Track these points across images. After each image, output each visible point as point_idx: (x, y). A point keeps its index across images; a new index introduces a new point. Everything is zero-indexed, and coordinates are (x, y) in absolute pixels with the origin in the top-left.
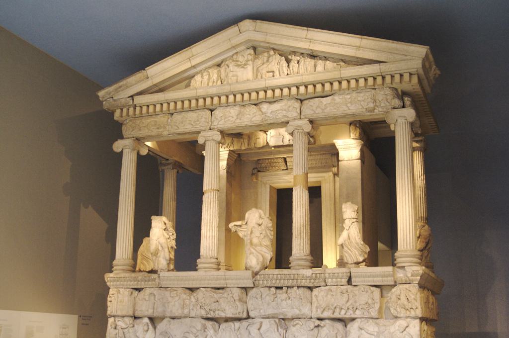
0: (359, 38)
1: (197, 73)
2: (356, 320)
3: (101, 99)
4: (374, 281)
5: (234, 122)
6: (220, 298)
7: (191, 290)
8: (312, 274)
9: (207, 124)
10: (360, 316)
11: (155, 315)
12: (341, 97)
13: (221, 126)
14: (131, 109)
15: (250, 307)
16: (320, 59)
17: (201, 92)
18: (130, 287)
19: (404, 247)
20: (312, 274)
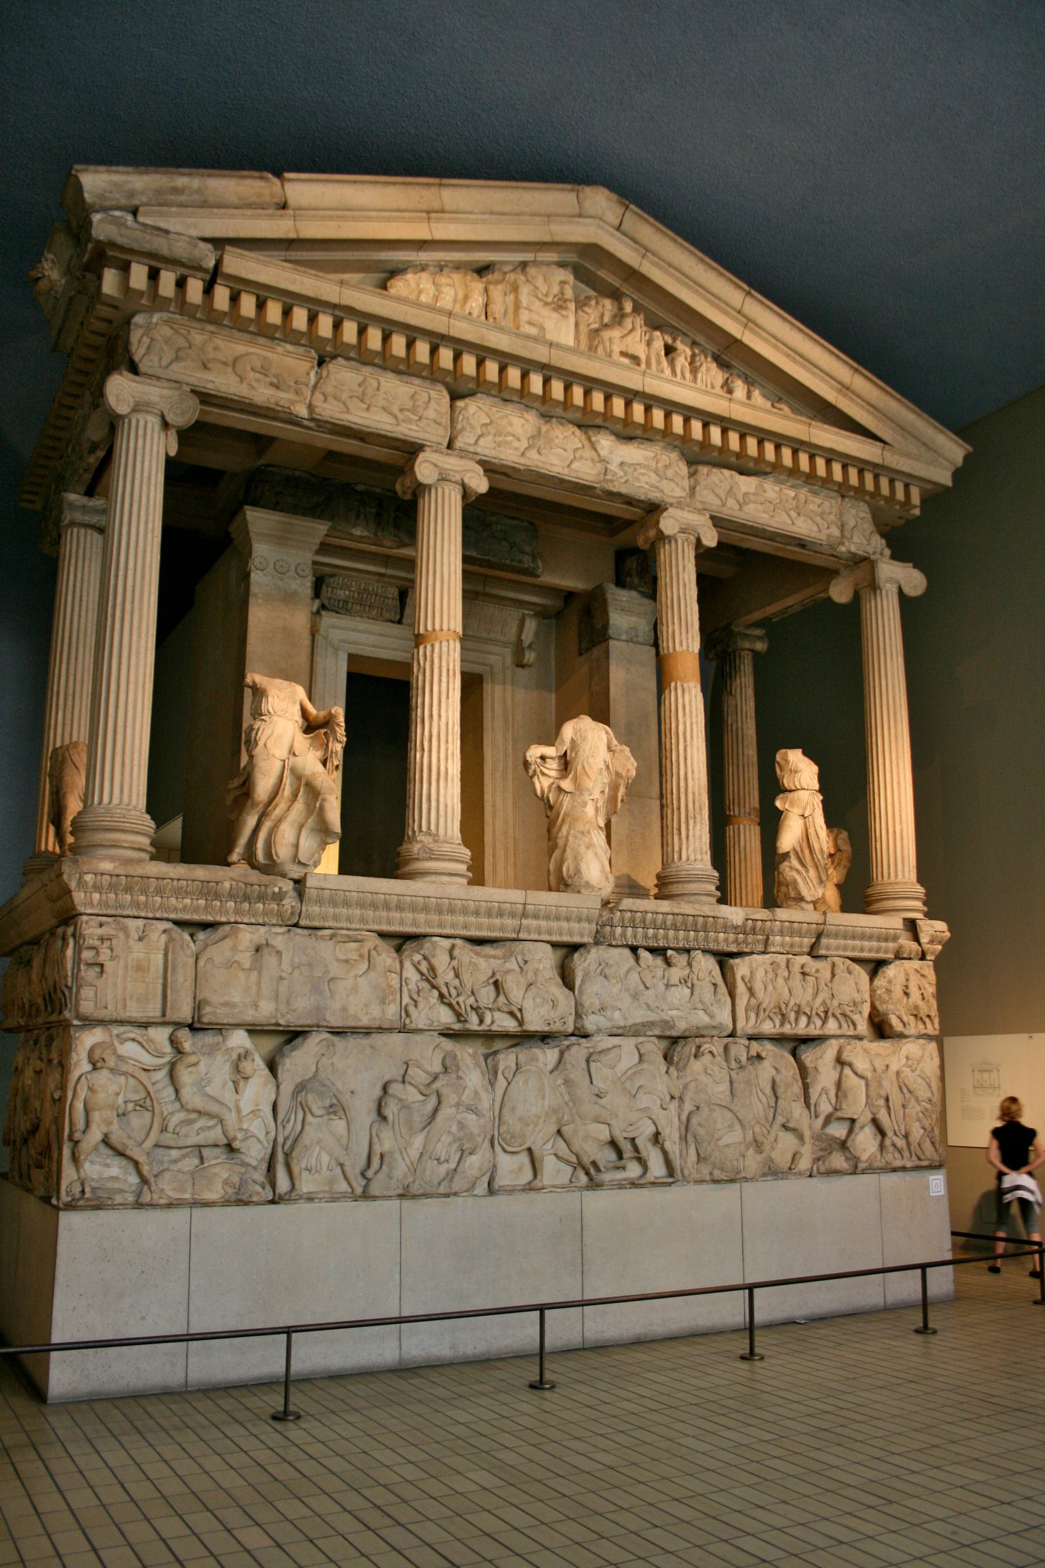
0: (852, 367)
2: (828, 1042)
3: (86, 195)
4: (862, 950)
5: (523, 454)
6: (508, 972)
7: (403, 942)
8: (747, 919)
9: (441, 431)
10: (839, 1032)
11: (282, 1022)
12: (777, 489)
13: (486, 452)
14: (195, 289)
15: (590, 1000)
16: (739, 376)
17: (461, 330)
18: (173, 916)
19: (904, 876)
20: (747, 919)
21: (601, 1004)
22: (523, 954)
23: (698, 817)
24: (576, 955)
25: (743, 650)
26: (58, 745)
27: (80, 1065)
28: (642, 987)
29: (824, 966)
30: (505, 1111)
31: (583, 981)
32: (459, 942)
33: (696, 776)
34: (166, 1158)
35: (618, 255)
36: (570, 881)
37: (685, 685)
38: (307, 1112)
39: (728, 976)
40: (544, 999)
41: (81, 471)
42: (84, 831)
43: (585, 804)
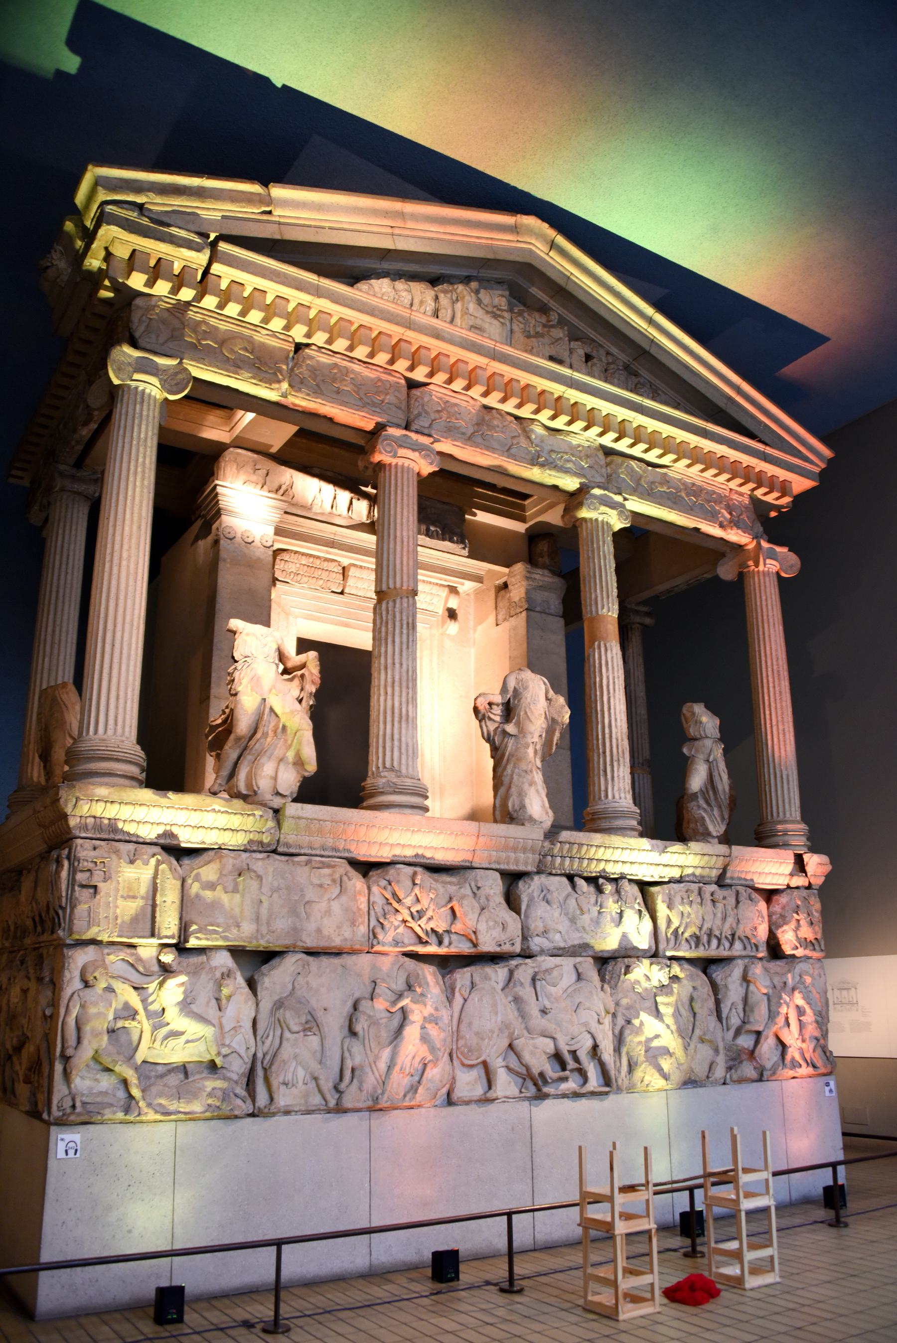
1: (379, 275)
2: (735, 962)
10: (744, 953)
15: (536, 925)
21: (545, 927)
22: (476, 881)
23: (621, 760)
24: (521, 884)
25: (634, 623)
26: (44, 687)
27: (72, 983)
28: (578, 912)
29: (730, 894)
30: (463, 1027)
31: (528, 906)
32: (419, 870)
33: (619, 724)
34: (153, 1074)
35: (548, 274)
36: (515, 815)
37: (608, 645)
38: (285, 1028)
39: (650, 903)
40: (496, 922)
41: (73, 443)
42: (79, 760)
43: (527, 746)
